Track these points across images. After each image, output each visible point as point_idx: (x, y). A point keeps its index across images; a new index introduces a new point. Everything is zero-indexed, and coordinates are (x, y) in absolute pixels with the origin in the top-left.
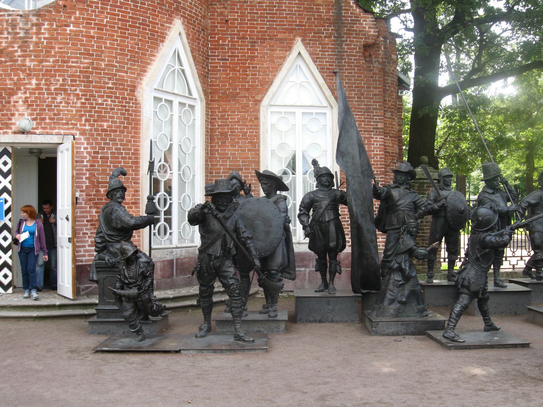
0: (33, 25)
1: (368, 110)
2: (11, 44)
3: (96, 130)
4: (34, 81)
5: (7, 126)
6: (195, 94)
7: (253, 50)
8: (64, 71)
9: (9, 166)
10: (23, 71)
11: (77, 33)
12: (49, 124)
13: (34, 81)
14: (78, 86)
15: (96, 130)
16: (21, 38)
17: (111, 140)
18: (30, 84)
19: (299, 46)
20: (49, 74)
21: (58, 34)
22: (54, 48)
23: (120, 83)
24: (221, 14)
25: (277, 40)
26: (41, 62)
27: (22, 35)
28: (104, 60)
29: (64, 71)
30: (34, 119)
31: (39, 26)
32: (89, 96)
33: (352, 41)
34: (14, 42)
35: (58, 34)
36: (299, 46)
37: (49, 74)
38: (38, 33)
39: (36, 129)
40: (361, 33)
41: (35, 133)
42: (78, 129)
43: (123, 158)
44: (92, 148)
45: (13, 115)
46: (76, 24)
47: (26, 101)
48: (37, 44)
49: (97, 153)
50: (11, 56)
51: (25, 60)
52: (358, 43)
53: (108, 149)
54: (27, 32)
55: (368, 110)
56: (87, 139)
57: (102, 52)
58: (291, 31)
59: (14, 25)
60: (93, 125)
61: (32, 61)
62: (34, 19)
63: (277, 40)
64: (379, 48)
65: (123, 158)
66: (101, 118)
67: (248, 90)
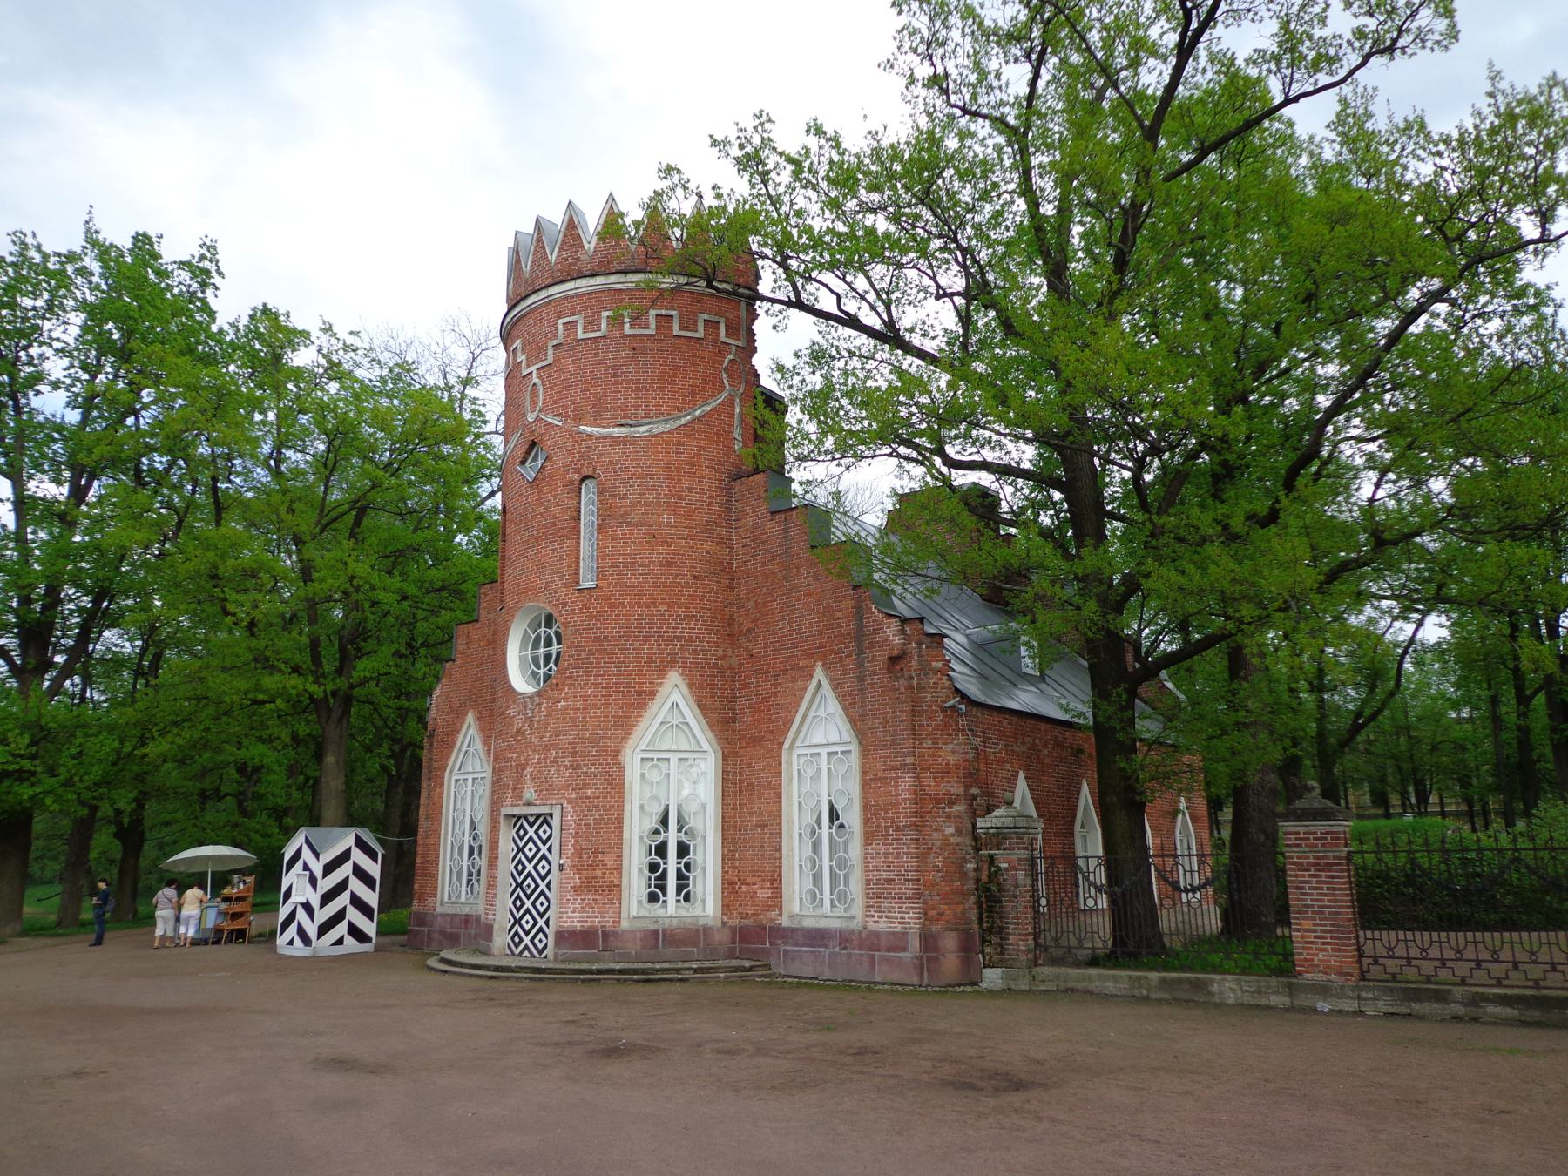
1: (893, 742)
6: (706, 746)
7: (775, 684)
11: (566, 708)
19: (819, 674)
23: (603, 750)
24: (747, 649)
25: (798, 669)
31: (540, 704)
32: (576, 766)
33: (874, 656)
36: (819, 674)
37: (546, 749)
40: (886, 643)
46: (566, 699)
52: (882, 657)
55: (893, 742)
56: (573, 807)
58: (811, 656)
62: (537, 699)
63: (798, 669)
64: (912, 657)
66: (585, 786)
67: (772, 732)
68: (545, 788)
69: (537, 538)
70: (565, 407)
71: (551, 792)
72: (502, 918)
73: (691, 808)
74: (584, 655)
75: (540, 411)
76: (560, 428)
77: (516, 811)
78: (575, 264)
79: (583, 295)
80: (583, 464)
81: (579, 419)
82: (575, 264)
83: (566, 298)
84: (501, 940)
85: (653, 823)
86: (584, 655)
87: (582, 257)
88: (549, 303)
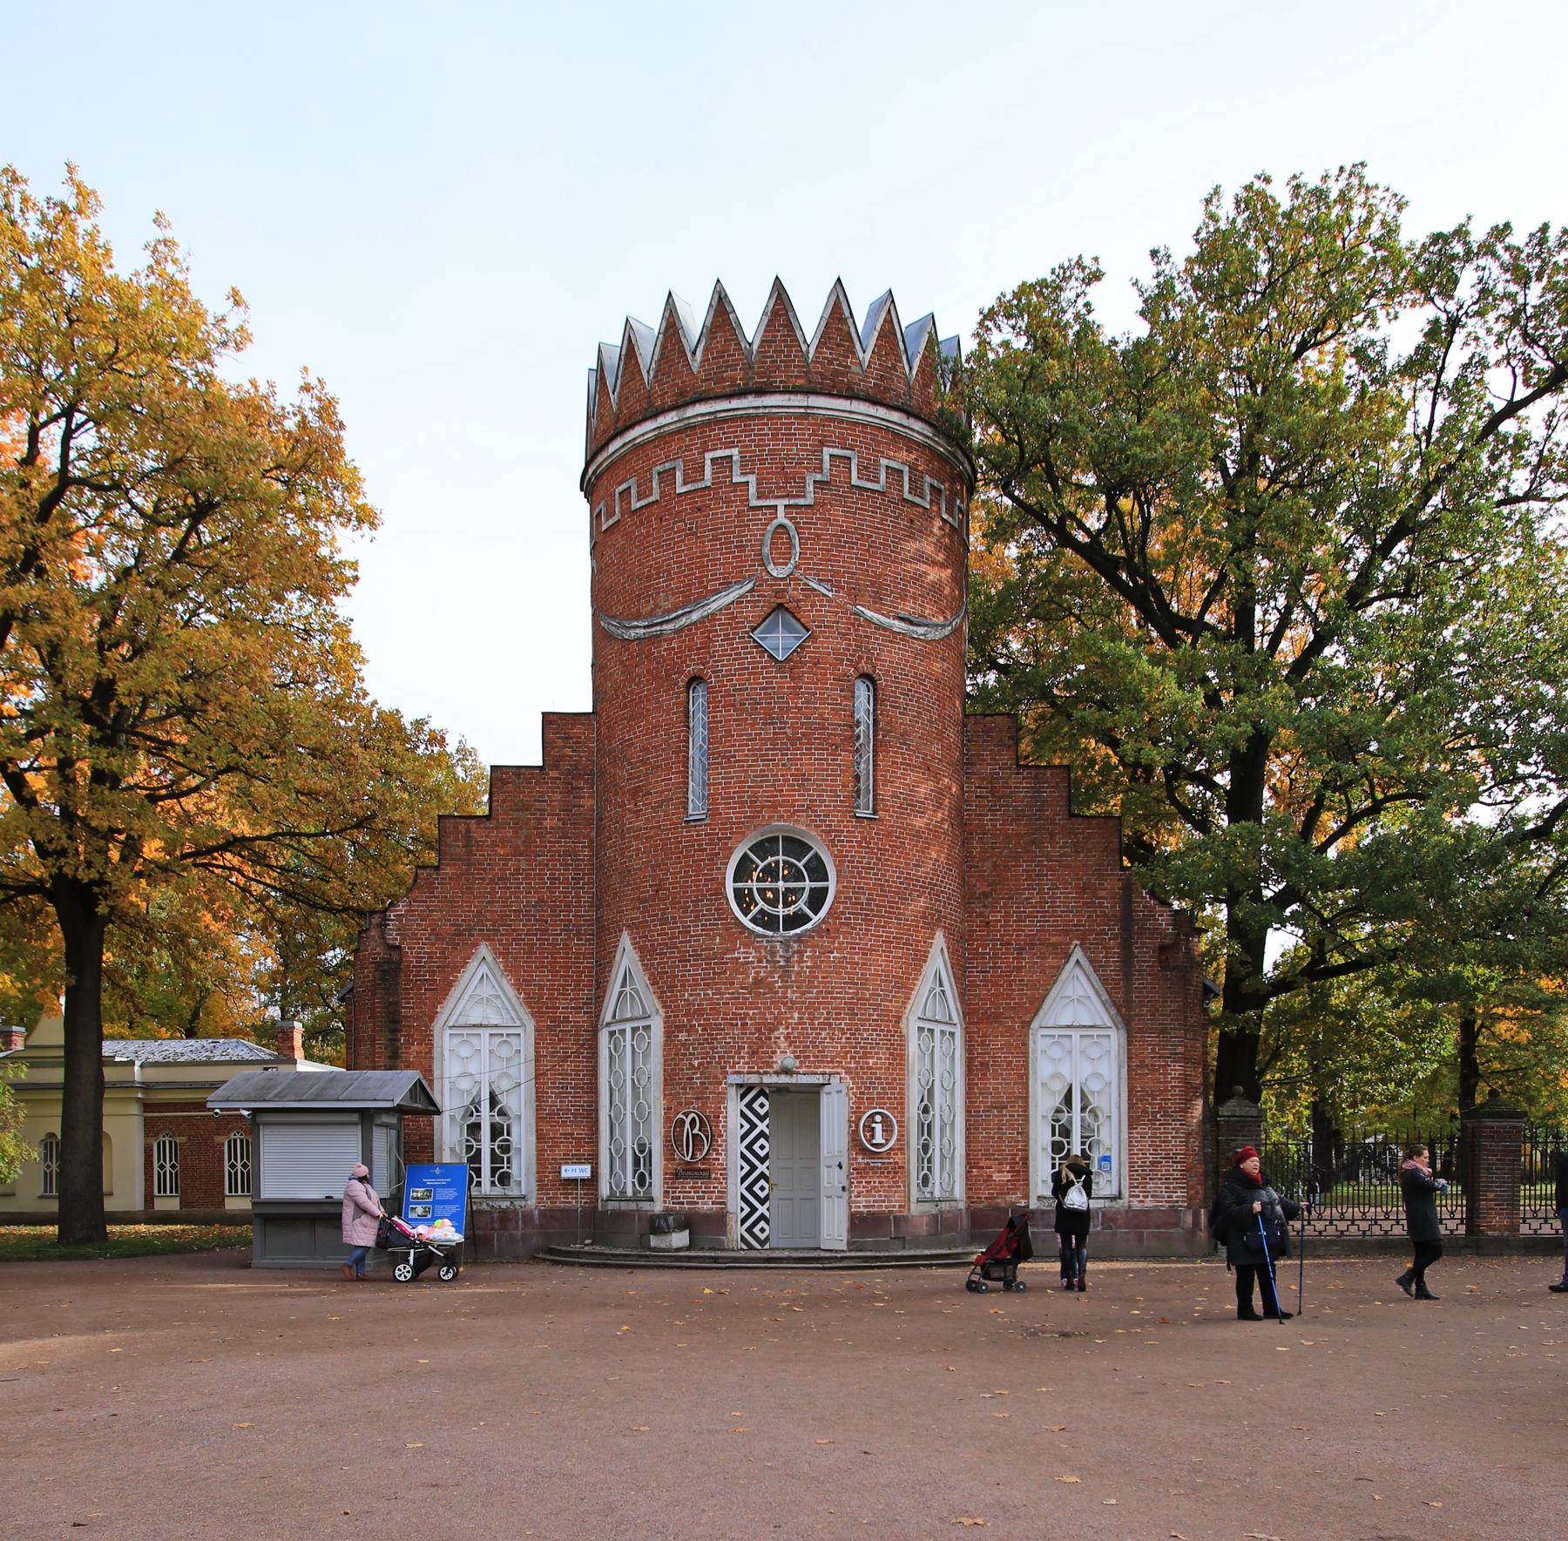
0: (794, 952)
2: (771, 974)
3: (862, 1068)
4: (796, 1015)
5: (769, 1065)
8: (828, 1003)
9: (766, 1108)
10: (785, 1004)
12: (814, 1062)
13: (796, 1015)
14: (844, 1019)
15: (862, 1068)
16: (781, 967)
17: (877, 1078)
18: (792, 1018)
20: (812, 1007)
21: (822, 962)
22: (817, 977)
26: (804, 993)
27: (782, 964)
28: (868, 989)
29: (828, 1003)
30: (797, 1057)
34: (774, 972)
35: (822, 962)
37: (812, 1007)
38: (800, 961)
39: (801, 1067)
41: (798, 1073)
42: (843, 1068)
43: (889, 1098)
44: (858, 1088)
45: (774, 1052)
46: (840, 950)
47: (787, 1037)
48: (798, 973)
49: (863, 1093)
50: (770, 986)
51: (786, 992)
53: (874, 1088)
54: (788, 960)
57: (867, 979)
59: (773, 953)
60: (858, 1063)
61: (794, 992)
62: (796, 946)
65: (889, 1098)
66: (866, 1056)
68: (807, 1052)
69: (793, 740)
70: (836, 574)
71: (821, 1059)
72: (736, 1208)
73: (1094, 1086)
74: (863, 899)
75: (797, 567)
76: (830, 601)
77: (754, 1079)
78: (843, 374)
79: (856, 424)
80: (861, 658)
81: (855, 594)
82: (843, 374)
83: (832, 419)
84: (736, 1230)
85: (1057, 1101)
86: (863, 899)
87: (855, 369)
88: (805, 416)
